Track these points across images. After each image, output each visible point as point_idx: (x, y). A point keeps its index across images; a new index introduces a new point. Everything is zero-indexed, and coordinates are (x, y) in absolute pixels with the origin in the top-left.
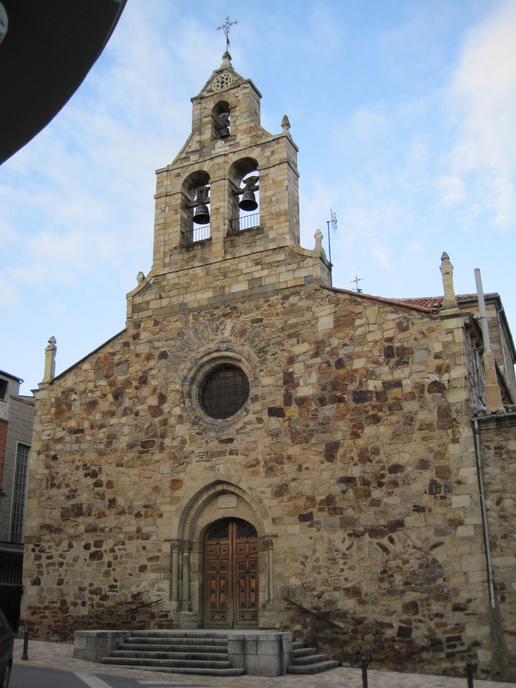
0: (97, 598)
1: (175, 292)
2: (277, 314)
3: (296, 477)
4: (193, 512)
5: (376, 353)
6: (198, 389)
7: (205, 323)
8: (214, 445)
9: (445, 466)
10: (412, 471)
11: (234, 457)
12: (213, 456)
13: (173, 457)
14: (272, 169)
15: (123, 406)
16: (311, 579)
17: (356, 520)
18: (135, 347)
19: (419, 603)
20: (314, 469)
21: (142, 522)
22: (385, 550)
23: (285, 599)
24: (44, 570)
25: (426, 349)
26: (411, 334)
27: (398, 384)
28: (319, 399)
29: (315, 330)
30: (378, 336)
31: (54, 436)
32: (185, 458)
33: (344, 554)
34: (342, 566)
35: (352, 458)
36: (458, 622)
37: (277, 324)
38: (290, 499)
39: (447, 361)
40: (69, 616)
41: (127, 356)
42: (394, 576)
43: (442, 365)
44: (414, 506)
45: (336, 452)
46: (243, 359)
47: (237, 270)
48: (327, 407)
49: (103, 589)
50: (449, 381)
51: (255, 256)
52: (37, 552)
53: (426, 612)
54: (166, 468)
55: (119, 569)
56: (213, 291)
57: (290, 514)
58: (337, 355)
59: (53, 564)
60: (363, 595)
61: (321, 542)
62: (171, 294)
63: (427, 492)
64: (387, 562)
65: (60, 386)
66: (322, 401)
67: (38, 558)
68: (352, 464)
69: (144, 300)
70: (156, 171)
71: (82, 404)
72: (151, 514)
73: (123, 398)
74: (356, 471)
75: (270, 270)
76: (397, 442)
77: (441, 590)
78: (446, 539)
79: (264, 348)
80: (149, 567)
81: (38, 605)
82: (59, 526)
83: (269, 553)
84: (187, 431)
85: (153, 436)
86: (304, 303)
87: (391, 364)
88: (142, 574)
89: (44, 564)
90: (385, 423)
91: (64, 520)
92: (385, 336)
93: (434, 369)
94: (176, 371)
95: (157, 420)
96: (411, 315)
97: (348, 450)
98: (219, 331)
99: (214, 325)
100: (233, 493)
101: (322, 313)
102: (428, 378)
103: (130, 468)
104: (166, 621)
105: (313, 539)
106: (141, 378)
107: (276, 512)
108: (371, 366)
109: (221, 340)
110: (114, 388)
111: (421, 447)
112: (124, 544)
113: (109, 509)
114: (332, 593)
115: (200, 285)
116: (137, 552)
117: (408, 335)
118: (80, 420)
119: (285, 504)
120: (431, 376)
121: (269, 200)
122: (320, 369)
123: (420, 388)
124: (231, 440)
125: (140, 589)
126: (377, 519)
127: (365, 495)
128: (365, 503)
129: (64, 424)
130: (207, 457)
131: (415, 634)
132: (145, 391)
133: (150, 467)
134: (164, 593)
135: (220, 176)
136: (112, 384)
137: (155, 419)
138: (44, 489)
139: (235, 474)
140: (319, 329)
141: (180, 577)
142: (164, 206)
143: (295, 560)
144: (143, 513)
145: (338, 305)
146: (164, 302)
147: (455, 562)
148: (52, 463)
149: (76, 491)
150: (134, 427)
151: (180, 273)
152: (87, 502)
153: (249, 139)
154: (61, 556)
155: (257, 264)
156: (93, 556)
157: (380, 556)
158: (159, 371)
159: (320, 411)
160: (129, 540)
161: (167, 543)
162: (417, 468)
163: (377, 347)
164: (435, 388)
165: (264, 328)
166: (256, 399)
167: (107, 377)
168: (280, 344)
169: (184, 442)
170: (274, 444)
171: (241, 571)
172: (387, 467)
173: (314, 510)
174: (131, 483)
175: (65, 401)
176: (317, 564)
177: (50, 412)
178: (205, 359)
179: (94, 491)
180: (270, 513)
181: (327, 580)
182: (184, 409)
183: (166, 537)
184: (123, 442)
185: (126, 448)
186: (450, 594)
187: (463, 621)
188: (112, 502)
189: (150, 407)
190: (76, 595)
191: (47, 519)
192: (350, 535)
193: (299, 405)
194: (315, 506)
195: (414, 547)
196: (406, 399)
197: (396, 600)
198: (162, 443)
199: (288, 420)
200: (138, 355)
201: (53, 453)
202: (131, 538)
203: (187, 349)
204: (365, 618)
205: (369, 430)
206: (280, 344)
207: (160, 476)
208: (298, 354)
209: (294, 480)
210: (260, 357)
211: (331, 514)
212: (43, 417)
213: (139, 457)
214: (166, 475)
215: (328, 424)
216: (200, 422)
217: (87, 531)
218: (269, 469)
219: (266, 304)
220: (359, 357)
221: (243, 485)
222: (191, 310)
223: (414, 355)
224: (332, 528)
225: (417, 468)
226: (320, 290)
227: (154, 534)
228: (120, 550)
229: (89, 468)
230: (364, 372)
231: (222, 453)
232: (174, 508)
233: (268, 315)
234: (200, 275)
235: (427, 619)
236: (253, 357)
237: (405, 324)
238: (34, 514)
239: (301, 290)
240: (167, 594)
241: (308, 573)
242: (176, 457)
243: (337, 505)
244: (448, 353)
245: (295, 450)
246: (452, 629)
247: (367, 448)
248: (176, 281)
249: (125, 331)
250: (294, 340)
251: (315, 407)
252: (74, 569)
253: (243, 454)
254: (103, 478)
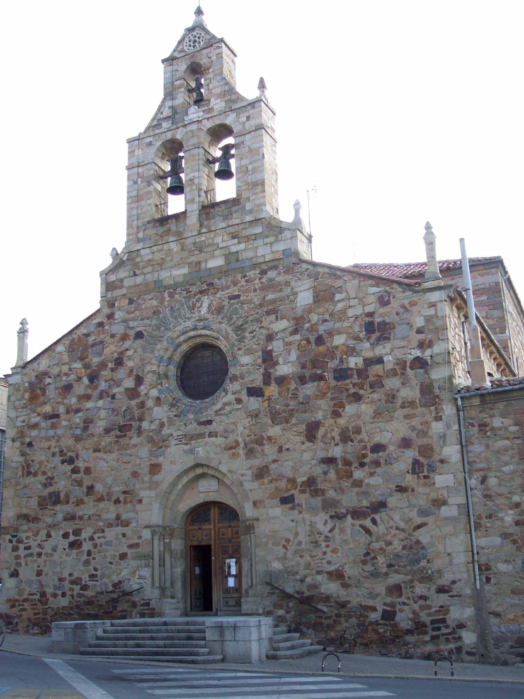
0: (77, 588)
1: (149, 269)
2: (255, 290)
3: (277, 459)
4: (173, 497)
5: (357, 328)
6: (176, 369)
7: (181, 301)
8: (193, 428)
9: (428, 445)
10: (395, 450)
11: (214, 439)
12: (192, 438)
13: (151, 440)
14: (248, 137)
15: (99, 389)
16: (293, 563)
17: (338, 502)
18: (110, 327)
19: (403, 585)
20: (295, 450)
21: (121, 508)
22: (368, 531)
23: (268, 584)
24: (23, 561)
25: (408, 324)
26: (392, 308)
27: (380, 360)
28: (299, 377)
29: (294, 306)
30: (358, 311)
31: (28, 422)
32: (163, 441)
33: (326, 537)
34: (324, 549)
35: (333, 438)
36: (443, 604)
37: (255, 300)
38: (271, 482)
39: (430, 336)
40: (49, 607)
41: (102, 337)
42: (377, 558)
43: (425, 340)
44: (397, 486)
45: (317, 432)
46: (221, 337)
47: (213, 244)
48: (307, 385)
49: (83, 578)
50: (431, 356)
51: (231, 230)
52: (14, 543)
53: (410, 595)
54: (144, 452)
55: (98, 556)
56: (189, 267)
57: (272, 497)
58: (317, 331)
59: (31, 555)
60: (347, 578)
61: (303, 526)
62: (145, 271)
63: (410, 472)
64: (370, 544)
65: (33, 370)
66: (302, 380)
67: (15, 549)
68: (333, 444)
69: (118, 278)
70: (128, 140)
71: (56, 388)
72: (130, 500)
73: (99, 381)
74: (337, 452)
75: (247, 243)
76: (378, 421)
77: (425, 572)
78: (430, 520)
79: (242, 325)
80: (129, 555)
81: (17, 597)
82: (37, 514)
83: (251, 536)
84: (166, 414)
85: (130, 420)
86: (281, 278)
87: (372, 340)
88: (122, 561)
89: (22, 555)
90: (366, 401)
91: (41, 509)
92: (366, 311)
93: (416, 344)
94: (152, 352)
95: (133, 403)
96: (392, 288)
97: (329, 430)
98: (196, 309)
99: (191, 303)
100: (214, 476)
101: (301, 288)
102: (410, 354)
103: (108, 453)
104: (147, 609)
105: (295, 522)
106: (116, 359)
107: (257, 495)
108: (351, 343)
109: (197, 318)
110: (89, 371)
111: (403, 426)
112: (103, 531)
113: (87, 496)
114: (315, 576)
115: (175, 260)
116: (116, 539)
117: (390, 310)
118: (55, 404)
119: (267, 486)
120: (413, 352)
121: (246, 169)
122: (300, 346)
123: (402, 364)
124: (210, 422)
125: (120, 578)
126: (359, 501)
127: (346, 476)
128: (347, 484)
129: (38, 410)
130: (185, 440)
131: (399, 617)
132: (121, 373)
133: (128, 452)
134: (145, 580)
135: (194, 145)
136: (87, 366)
137: (131, 402)
138: (20, 477)
139: (215, 456)
140: (298, 305)
141: (162, 564)
142: (136, 177)
143: (278, 544)
144: (122, 499)
145: (317, 279)
146: (139, 280)
147: (439, 543)
148: (28, 450)
149: (52, 478)
150: (110, 410)
151: (155, 249)
152: (65, 489)
153: (223, 104)
154: (39, 546)
155: (234, 238)
156: (72, 545)
157: (363, 539)
158: (135, 352)
159: (300, 390)
160: (108, 527)
162: (400, 447)
163: (358, 323)
164: (418, 364)
165: (242, 304)
166: (234, 378)
167: (82, 359)
168: (259, 321)
169: (162, 425)
170: (254, 425)
172: (368, 447)
173: (296, 492)
174: (108, 469)
175: (39, 386)
176: (299, 548)
177: (23, 397)
178: (182, 338)
179: (71, 478)
180: (251, 496)
181: (310, 563)
182: (160, 391)
183: (146, 523)
184: (100, 426)
185: (102, 433)
186: (434, 576)
187: (447, 603)
188: (91, 488)
189: (127, 389)
190: (56, 586)
191: (24, 508)
192: (332, 517)
193: (278, 384)
194: (296, 488)
195: (397, 528)
196: (387, 376)
197: (380, 583)
198: (140, 427)
199: (267, 400)
200: (113, 336)
201: (28, 440)
202: (110, 525)
203: (163, 328)
204: (349, 602)
205: (350, 409)
206: (259, 321)
207: (138, 461)
208: (276, 331)
209: (275, 461)
210: (238, 336)
211: (312, 496)
212: (17, 402)
213: (116, 442)
215: (308, 403)
216: (179, 404)
217: (65, 519)
218: (249, 450)
219: (244, 280)
220: (340, 333)
221: (223, 468)
222: (166, 288)
223: (396, 330)
224: (313, 510)
225: (400, 447)
226: (298, 264)
227: (134, 520)
228: (99, 538)
229: (65, 454)
230: (345, 349)
231: (201, 436)
232: (153, 493)
233: (246, 291)
234: (175, 250)
235: (411, 602)
236: (231, 335)
237: (387, 299)
238: (10, 505)
239: (279, 264)
240: (149, 582)
241: (291, 557)
242: (154, 441)
243: (319, 487)
244: (431, 327)
245: (275, 431)
246: (436, 611)
247: (348, 428)
248: (150, 257)
249: (98, 311)
250: (273, 317)
251: (295, 386)
252: (53, 559)
253: (221, 436)
254: (81, 464)
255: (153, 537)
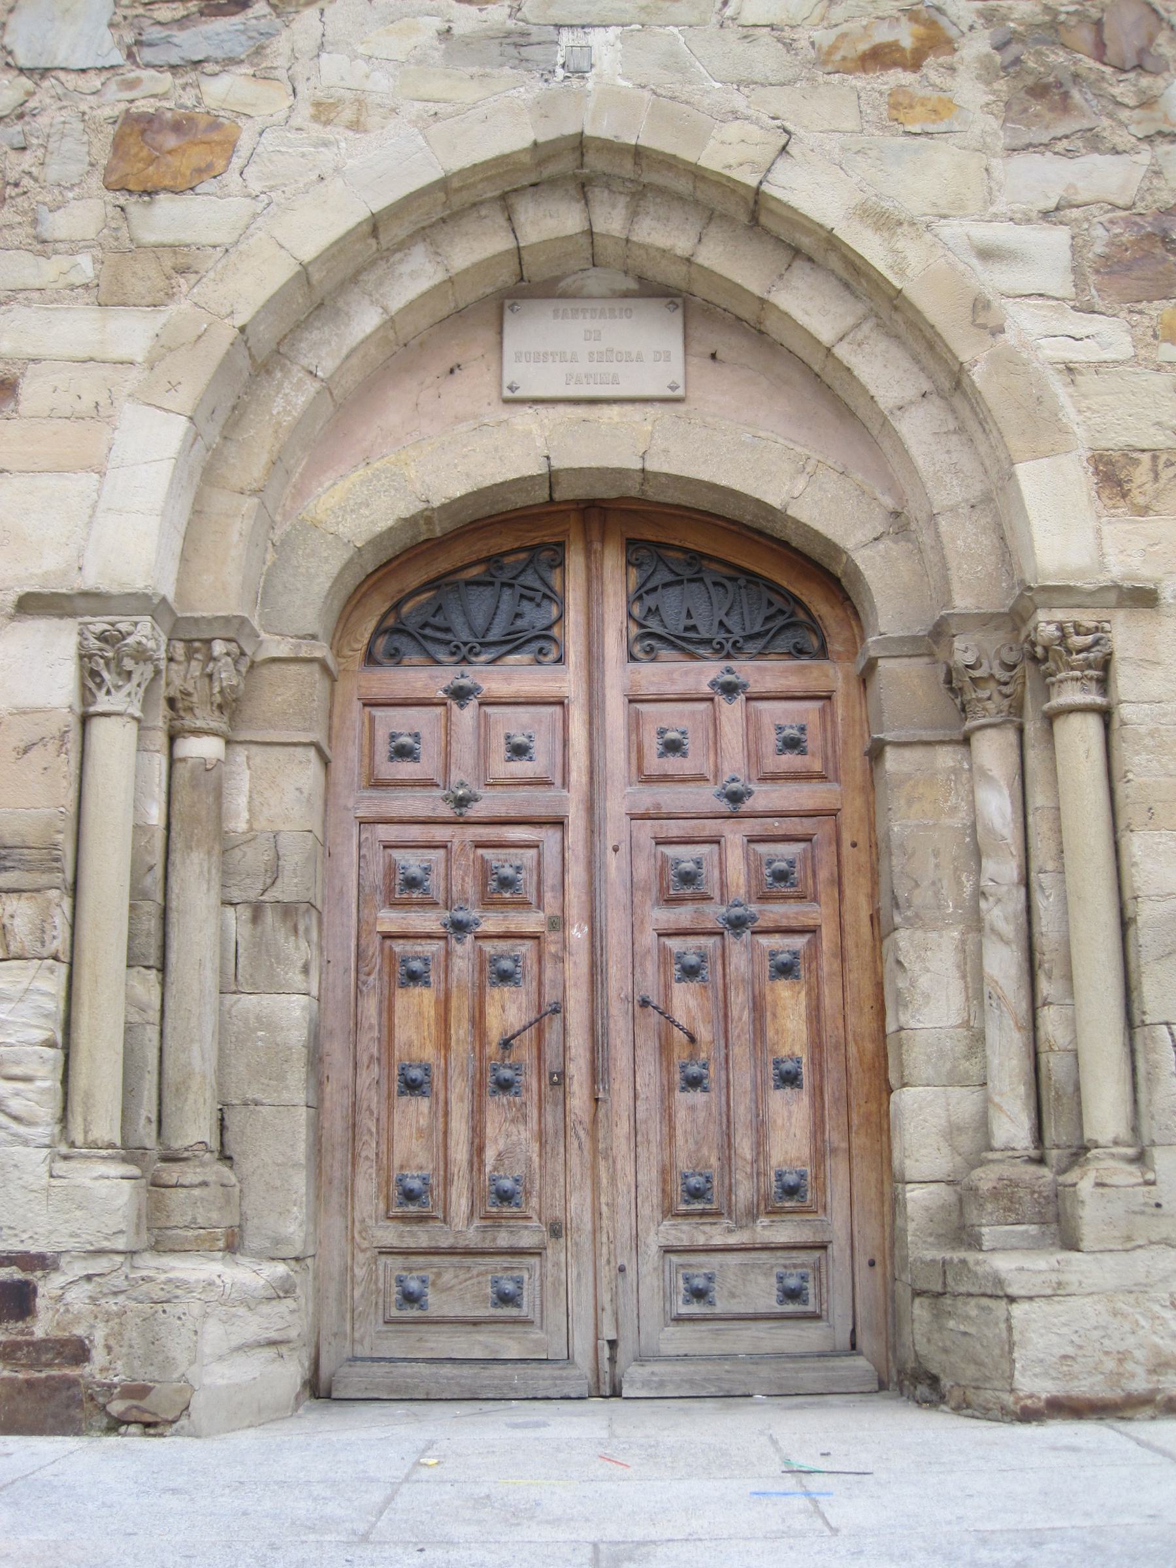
139: (739, 102)
161: (38, 629)
171: (683, 915)
180: (1070, 415)
214: (71, 80)
255: (86, 695)
